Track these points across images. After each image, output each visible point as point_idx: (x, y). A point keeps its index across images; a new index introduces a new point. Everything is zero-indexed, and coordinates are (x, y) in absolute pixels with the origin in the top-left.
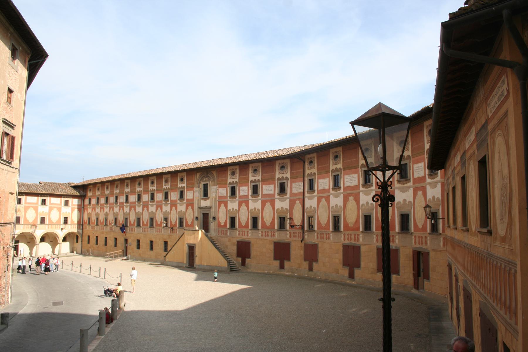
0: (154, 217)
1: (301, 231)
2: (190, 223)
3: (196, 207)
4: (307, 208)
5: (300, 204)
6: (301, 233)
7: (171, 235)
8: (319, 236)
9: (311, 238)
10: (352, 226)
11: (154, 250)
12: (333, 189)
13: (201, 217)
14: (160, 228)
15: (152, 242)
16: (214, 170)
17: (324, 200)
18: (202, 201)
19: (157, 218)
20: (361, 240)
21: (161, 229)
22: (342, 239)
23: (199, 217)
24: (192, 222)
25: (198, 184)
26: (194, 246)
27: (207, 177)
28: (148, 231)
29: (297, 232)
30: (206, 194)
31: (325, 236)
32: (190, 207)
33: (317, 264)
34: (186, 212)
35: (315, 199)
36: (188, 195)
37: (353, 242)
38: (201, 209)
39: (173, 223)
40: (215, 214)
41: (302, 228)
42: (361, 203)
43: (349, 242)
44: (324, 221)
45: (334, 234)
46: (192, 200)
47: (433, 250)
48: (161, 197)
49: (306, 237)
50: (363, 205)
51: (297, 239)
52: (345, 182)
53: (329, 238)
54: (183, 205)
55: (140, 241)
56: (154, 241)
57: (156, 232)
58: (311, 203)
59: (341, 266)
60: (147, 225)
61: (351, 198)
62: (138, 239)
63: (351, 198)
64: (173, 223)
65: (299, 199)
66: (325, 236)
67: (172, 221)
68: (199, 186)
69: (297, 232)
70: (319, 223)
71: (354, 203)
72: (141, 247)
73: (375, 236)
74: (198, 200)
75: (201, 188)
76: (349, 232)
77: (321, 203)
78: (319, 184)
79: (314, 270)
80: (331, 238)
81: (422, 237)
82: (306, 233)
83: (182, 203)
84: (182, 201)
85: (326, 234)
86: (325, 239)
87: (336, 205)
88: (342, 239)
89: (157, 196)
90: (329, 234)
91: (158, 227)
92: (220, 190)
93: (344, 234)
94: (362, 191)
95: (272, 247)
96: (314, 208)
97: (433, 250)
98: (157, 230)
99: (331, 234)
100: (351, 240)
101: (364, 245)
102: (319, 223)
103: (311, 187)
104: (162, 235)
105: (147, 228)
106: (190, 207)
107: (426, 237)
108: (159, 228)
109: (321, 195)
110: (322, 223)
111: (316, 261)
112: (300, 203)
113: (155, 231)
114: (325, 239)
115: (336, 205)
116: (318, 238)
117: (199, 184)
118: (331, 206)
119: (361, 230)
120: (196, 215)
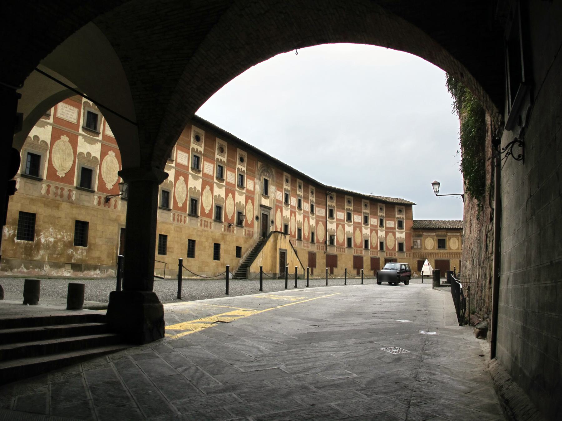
0: (199, 199)
1: (323, 245)
2: (249, 222)
3: (256, 204)
4: (329, 229)
5: (322, 225)
6: (323, 246)
7: (225, 235)
8: (338, 250)
9: (332, 251)
10: (359, 245)
11: (196, 257)
12: (347, 221)
13: (260, 217)
14: (209, 220)
15: (192, 244)
16: (274, 168)
17: (340, 226)
18: (263, 199)
19: (204, 203)
20: (363, 253)
21: (211, 223)
22: (353, 252)
23: (259, 217)
24: (252, 222)
25: (259, 176)
26: (285, 253)
27: (267, 172)
28: (185, 222)
29: (321, 246)
30: (266, 192)
31: (342, 250)
32: (250, 201)
33: (337, 269)
34: (246, 207)
35: (335, 224)
36: (249, 184)
37: (359, 254)
38: (262, 208)
39: (230, 217)
40: (273, 217)
41: (326, 242)
42: (363, 233)
43: (357, 254)
44: (341, 240)
45: (348, 249)
46: (253, 193)
47: (400, 258)
48: (212, 170)
49: (328, 250)
50: (364, 234)
51: (321, 251)
52: (355, 219)
53: (345, 251)
54: (242, 195)
55: (169, 239)
56: (196, 241)
57: (201, 225)
58: (332, 226)
59: (352, 268)
60: (183, 209)
61: (358, 229)
62: (163, 233)
63: (358, 229)
64: (230, 217)
65: (322, 221)
66: (342, 250)
67: (228, 215)
68: (260, 180)
69: (321, 246)
70: (338, 241)
71: (359, 232)
72: (168, 251)
73: (370, 251)
74: (259, 195)
75: (262, 183)
76: (357, 249)
77: (339, 228)
78: (337, 215)
79: (334, 273)
80: (346, 251)
81: (392, 253)
82: (328, 247)
83: (241, 192)
84: (241, 189)
85: (343, 248)
86: (342, 252)
87: (366, 233)
88: (353, 252)
89: (205, 166)
90: (344, 249)
91: (204, 219)
92: (278, 192)
93: (354, 250)
94: (364, 227)
95: (307, 256)
96: (334, 230)
97: (400, 258)
98: (203, 222)
99: (346, 249)
100: (358, 253)
101: (365, 256)
102: (338, 241)
103: (332, 215)
104: (212, 232)
105: (183, 216)
106: (250, 201)
107: (395, 253)
108: (206, 220)
109: (339, 222)
110: (340, 241)
111: (336, 267)
112: (323, 224)
113: (199, 224)
114: (342, 252)
115: (349, 231)
116: (337, 251)
117: (260, 176)
118: (346, 231)
119: (363, 248)
120: (256, 213)
